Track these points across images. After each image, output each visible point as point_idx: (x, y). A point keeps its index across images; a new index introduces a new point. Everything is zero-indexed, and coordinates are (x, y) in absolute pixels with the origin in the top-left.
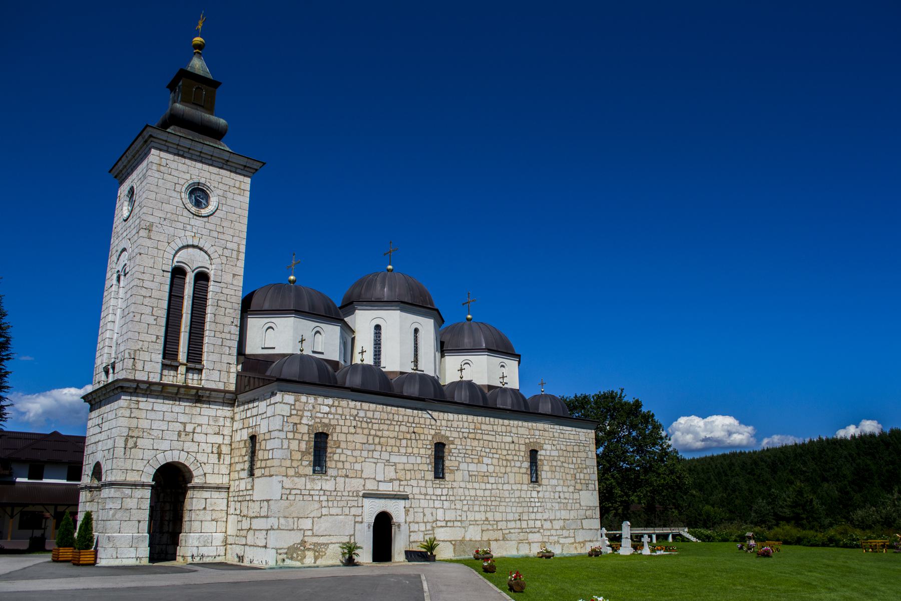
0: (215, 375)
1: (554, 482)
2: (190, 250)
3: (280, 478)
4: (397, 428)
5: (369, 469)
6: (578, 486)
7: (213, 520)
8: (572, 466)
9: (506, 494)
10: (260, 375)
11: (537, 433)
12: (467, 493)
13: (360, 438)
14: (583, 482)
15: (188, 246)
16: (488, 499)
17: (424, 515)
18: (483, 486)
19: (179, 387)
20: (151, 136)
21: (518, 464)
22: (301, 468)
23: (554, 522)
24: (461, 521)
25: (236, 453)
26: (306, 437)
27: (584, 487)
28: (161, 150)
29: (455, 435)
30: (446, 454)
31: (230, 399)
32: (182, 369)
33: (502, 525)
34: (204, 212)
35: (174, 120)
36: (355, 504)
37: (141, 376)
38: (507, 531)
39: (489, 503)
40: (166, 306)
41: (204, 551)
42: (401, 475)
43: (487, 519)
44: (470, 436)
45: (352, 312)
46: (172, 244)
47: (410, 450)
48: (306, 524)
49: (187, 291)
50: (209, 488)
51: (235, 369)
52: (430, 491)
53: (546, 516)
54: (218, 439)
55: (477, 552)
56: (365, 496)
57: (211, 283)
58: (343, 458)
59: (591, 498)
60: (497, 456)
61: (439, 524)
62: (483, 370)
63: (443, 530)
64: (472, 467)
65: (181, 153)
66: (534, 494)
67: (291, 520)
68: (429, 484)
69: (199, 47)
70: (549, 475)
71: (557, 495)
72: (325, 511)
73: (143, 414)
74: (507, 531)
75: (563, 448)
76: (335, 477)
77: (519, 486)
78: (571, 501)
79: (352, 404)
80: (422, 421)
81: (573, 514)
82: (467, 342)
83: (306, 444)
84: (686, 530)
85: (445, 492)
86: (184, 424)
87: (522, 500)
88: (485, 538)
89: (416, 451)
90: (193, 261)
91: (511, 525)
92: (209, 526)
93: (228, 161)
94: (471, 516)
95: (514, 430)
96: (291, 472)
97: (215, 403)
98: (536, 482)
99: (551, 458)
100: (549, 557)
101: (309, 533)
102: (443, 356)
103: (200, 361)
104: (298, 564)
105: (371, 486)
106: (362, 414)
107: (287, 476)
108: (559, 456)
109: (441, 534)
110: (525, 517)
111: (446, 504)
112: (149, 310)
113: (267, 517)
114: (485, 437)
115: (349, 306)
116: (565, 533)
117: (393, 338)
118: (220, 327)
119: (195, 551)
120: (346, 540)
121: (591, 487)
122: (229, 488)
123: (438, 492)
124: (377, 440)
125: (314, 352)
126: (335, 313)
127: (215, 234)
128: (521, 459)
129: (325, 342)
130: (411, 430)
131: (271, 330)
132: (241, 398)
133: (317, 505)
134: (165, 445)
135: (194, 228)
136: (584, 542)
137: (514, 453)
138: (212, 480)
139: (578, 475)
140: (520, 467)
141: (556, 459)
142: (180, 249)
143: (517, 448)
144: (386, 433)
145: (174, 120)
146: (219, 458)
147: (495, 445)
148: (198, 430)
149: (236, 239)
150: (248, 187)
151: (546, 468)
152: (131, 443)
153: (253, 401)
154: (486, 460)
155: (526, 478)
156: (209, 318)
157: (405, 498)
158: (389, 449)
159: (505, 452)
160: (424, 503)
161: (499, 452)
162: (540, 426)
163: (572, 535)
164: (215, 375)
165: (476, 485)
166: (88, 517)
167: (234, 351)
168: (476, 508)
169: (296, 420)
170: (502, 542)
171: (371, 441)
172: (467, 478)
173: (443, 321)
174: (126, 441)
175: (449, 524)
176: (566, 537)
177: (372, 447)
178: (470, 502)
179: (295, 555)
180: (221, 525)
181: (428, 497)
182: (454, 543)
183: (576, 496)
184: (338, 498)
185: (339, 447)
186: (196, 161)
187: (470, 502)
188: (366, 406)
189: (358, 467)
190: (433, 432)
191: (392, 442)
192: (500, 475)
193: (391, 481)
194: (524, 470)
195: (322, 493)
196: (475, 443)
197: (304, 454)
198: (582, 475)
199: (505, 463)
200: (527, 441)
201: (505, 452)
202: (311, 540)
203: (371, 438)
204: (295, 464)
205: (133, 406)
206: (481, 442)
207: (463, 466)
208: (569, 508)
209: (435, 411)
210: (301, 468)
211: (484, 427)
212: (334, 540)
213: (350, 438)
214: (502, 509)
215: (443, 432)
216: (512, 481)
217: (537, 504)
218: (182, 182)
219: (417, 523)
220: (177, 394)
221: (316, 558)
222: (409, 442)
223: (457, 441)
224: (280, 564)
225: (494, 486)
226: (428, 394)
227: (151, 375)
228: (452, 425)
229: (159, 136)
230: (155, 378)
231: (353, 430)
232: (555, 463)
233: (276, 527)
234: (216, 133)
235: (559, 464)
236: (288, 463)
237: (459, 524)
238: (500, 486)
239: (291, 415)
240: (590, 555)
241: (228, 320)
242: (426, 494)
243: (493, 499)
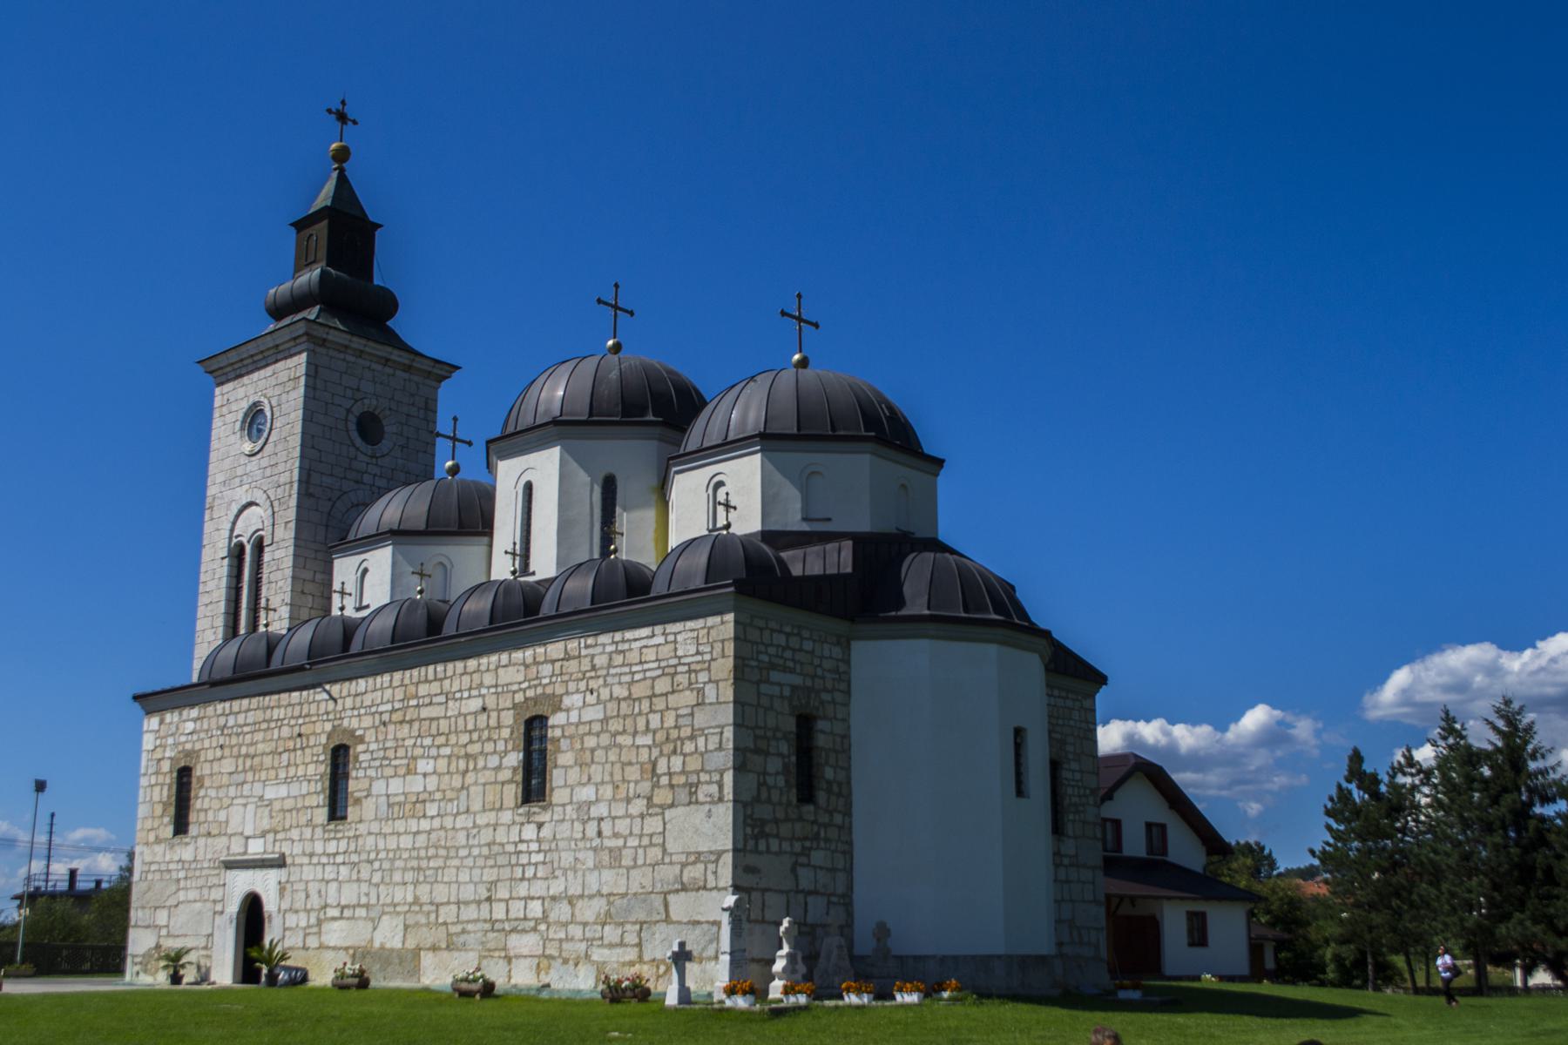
2: (246, 512)
8: (648, 740)
11: (546, 670)
13: (228, 765)
16: (423, 853)
18: (413, 825)
21: (493, 761)
23: (580, 904)
24: (367, 906)
27: (683, 796)
29: (367, 721)
33: (447, 914)
38: (458, 928)
43: (416, 901)
53: (557, 887)
56: (230, 865)
58: (206, 806)
63: (336, 925)
64: (396, 786)
68: (319, 831)
70: (574, 775)
71: (592, 829)
74: (458, 928)
75: (619, 692)
77: (490, 817)
78: (633, 842)
85: (343, 845)
87: (496, 849)
88: (411, 944)
91: (470, 913)
96: (152, 838)
99: (583, 729)
108: (605, 720)
111: (344, 871)
114: (425, 713)
123: (332, 847)
139: (662, 767)
140: (499, 768)
141: (596, 727)
144: (261, 747)
150: (302, 370)
151: (565, 758)
159: (464, 738)
160: (308, 873)
163: (631, 938)
165: (400, 826)
168: (397, 877)
170: (445, 954)
176: (611, 946)
178: (386, 865)
181: (315, 860)
183: (653, 824)
186: (252, 372)
189: (222, 816)
190: (328, 727)
192: (449, 794)
196: (404, 730)
197: (165, 805)
198: (677, 763)
199: (462, 764)
206: (416, 725)
207: (379, 787)
208: (627, 862)
209: (335, 681)
211: (423, 689)
214: (449, 875)
215: (346, 723)
216: (476, 806)
217: (536, 858)
219: (297, 912)
223: (370, 736)
225: (436, 823)
228: (362, 702)
242: (311, 855)
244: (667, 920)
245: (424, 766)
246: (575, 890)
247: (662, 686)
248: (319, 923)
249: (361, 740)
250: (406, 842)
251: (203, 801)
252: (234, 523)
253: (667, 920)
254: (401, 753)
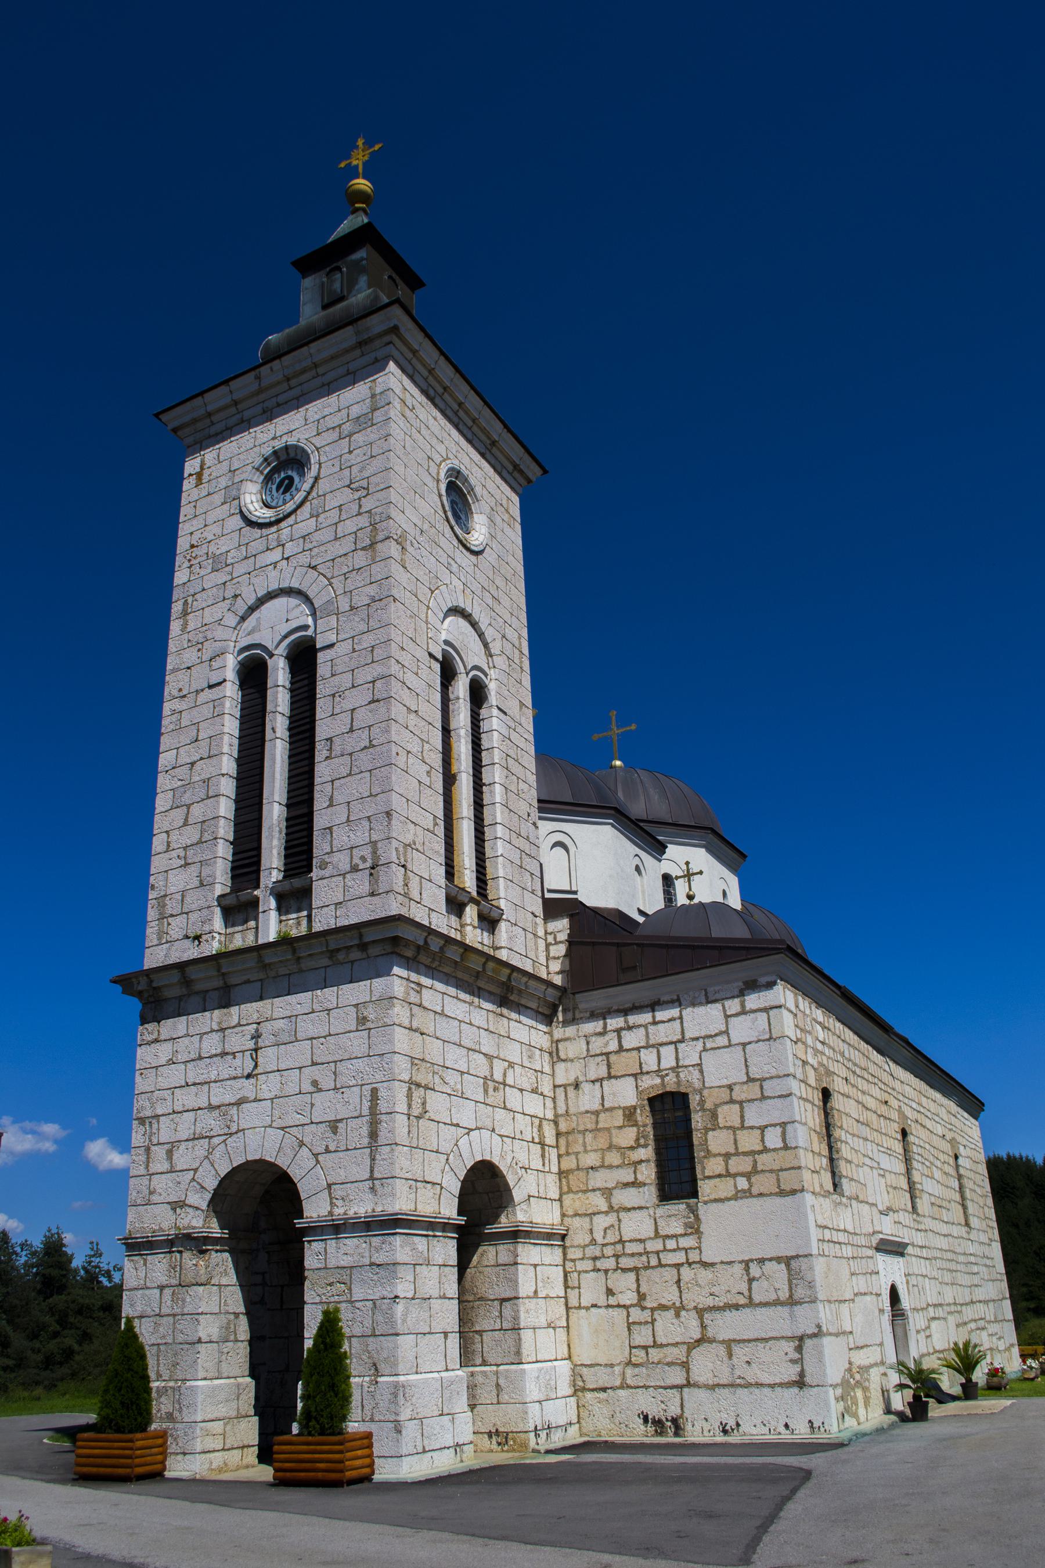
7: (549, 1326)
20: (395, 330)
28: (403, 370)
31: (552, 1005)
50: (539, 1235)
65: (432, 392)
93: (494, 443)
119: (535, 1416)
122: (563, 1237)
131: (558, 849)
153: (653, 1006)
166: (330, 1325)
174: (409, 1096)
205: (413, 998)
229: (408, 336)
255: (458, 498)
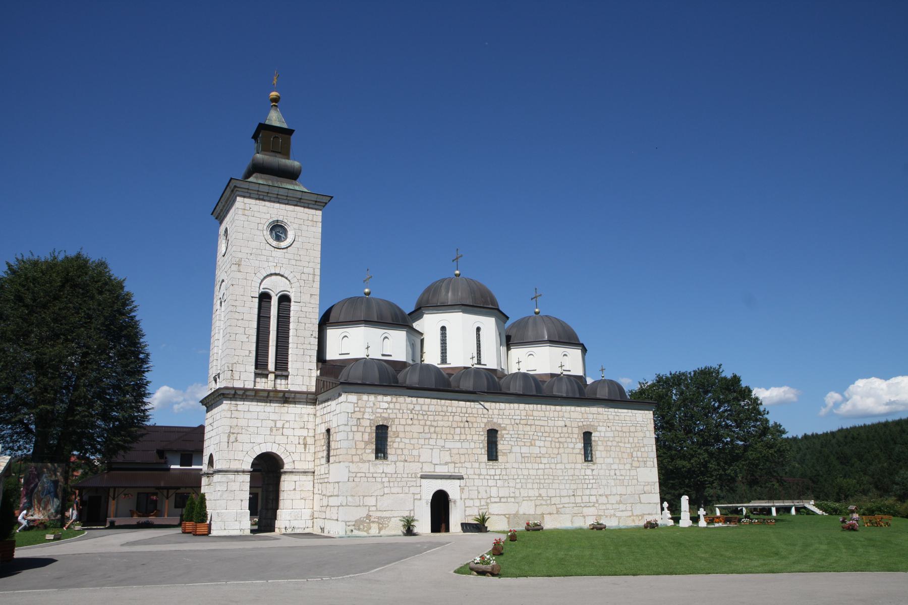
0: (299, 380)
1: (610, 460)
2: (273, 277)
3: (347, 464)
4: (451, 418)
5: (425, 455)
6: (635, 464)
8: (629, 445)
9: (560, 473)
10: (336, 377)
11: (591, 416)
12: (520, 472)
13: (417, 428)
14: (640, 459)
15: (271, 275)
16: (541, 477)
17: (479, 493)
18: (536, 466)
19: (269, 391)
21: (571, 445)
22: (365, 455)
23: (610, 497)
24: (514, 497)
25: (318, 443)
26: (368, 430)
27: (642, 464)
28: (244, 197)
29: (507, 422)
30: (499, 439)
31: (312, 399)
32: (271, 377)
33: (554, 501)
34: (283, 244)
35: (257, 168)
36: (412, 484)
37: (238, 384)
39: (542, 481)
40: (255, 326)
41: (295, 523)
42: (456, 458)
43: (540, 495)
44: (522, 422)
45: (420, 317)
46: (258, 274)
47: (463, 437)
48: (371, 501)
49: (272, 312)
51: (316, 373)
52: (484, 472)
54: (304, 433)
55: (528, 524)
56: (422, 477)
57: (292, 304)
58: (402, 445)
59: (651, 474)
60: (550, 439)
61: (493, 500)
62: (540, 360)
64: (525, 450)
66: (589, 472)
67: (357, 499)
68: (483, 465)
69: (276, 100)
70: (604, 454)
71: (612, 473)
72: (386, 490)
73: (241, 415)
76: (395, 462)
78: (627, 478)
79: (409, 400)
80: (474, 411)
81: (630, 490)
82: (530, 334)
83: (369, 435)
84: (812, 502)
86: (275, 421)
87: (575, 477)
88: (539, 512)
89: (469, 437)
90: (276, 287)
92: (299, 504)
94: (524, 493)
95: (567, 415)
97: (300, 402)
98: (591, 461)
99: (606, 439)
100: (601, 529)
101: (374, 508)
102: (508, 349)
103: (286, 369)
104: (365, 534)
105: (428, 469)
106: (418, 408)
107: (352, 462)
108: (614, 437)
109: (494, 509)
110: (579, 493)
112: (242, 330)
113: (338, 496)
114: (537, 423)
115: (418, 313)
116: (622, 507)
117: (459, 338)
118: (301, 340)
120: (406, 514)
121: (649, 464)
123: (492, 472)
124: (432, 429)
125: (383, 355)
126: (401, 320)
127: (293, 262)
128: (574, 440)
129: (391, 345)
130: (464, 419)
132: (320, 397)
133: (380, 486)
134: (260, 439)
135: (275, 258)
136: (643, 515)
137: (567, 435)
138: (300, 466)
140: (573, 448)
141: (611, 439)
142: (265, 278)
143: (570, 431)
144: (440, 424)
145: (257, 168)
146: (305, 448)
147: (547, 429)
148: (287, 425)
149: (311, 264)
150: (320, 219)
151: (600, 448)
152: (232, 438)
154: (538, 443)
155: (581, 458)
156: (291, 333)
157: (461, 478)
158: (444, 437)
159: (557, 435)
160: (478, 482)
161: (552, 435)
162: (594, 410)
163: (629, 508)
164: (299, 380)
165: (529, 466)
167: (315, 359)
168: (529, 486)
169: (359, 415)
171: (427, 431)
172: (520, 459)
173: (508, 318)
174: (229, 436)
175: (503, 500)
177: (428, 436)
178: (523, 481)
179: (361, 527)
180: (309, 503)
181: (482, 477)
182: (509, 517)
183: (633, 473)
184: (399, 480)
185: (398, 437)
186: (274, 202)
187: (523, 481)
188: (421, 400)
189: (415, 453)
190: (485, 420)
191: (447, 430)
193: (446, 463)
194: (578, 451)
195: (384, 475)
197: (367, 443)
198: (639, 454)
199: (557, 445)
200: (580, 424)
201: (557, 435)
202: (375, 514)
203: (426, 428)
204: (359, 452)
205: (233, 408)
206: (533, 427)
207: (516, 449)
210: (365, 455)
211: (535, 413)
212: (396, 514)
213: (408, 428)
214: (555, 486)
215: (495, 420)
216: (565, 461)
217: (591, 481)
218: (263, 221)
220: (268, 397)
221: (380, 529)
222: (463, 430)
224: (349, 533)
225: (547, 466)
226: (488, 386)
227: (246, 383)
230: (250, 385)
231: (410, 422)
232: (609, 444)
233: (344, 504)
234: (292, 175)
235: (615, 443)
236: (353, 451)
237: (513, 500)
238: (553, 466)
239: (355, 411)
240: (646, 527)
241: (308, 333)
243: (546, 477)
244: (640, 503)
245: (538, 443)
246: (608, 493)
247: (633, 429)
248: (487, 504)
249: (505, 429)
250: (531, 472)
251: (394, 445)
252: (262, 281)
253: (640, 503)
254: (526, 437)
255: (278, 230)
